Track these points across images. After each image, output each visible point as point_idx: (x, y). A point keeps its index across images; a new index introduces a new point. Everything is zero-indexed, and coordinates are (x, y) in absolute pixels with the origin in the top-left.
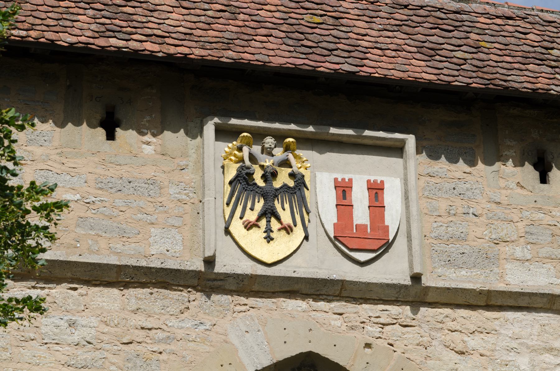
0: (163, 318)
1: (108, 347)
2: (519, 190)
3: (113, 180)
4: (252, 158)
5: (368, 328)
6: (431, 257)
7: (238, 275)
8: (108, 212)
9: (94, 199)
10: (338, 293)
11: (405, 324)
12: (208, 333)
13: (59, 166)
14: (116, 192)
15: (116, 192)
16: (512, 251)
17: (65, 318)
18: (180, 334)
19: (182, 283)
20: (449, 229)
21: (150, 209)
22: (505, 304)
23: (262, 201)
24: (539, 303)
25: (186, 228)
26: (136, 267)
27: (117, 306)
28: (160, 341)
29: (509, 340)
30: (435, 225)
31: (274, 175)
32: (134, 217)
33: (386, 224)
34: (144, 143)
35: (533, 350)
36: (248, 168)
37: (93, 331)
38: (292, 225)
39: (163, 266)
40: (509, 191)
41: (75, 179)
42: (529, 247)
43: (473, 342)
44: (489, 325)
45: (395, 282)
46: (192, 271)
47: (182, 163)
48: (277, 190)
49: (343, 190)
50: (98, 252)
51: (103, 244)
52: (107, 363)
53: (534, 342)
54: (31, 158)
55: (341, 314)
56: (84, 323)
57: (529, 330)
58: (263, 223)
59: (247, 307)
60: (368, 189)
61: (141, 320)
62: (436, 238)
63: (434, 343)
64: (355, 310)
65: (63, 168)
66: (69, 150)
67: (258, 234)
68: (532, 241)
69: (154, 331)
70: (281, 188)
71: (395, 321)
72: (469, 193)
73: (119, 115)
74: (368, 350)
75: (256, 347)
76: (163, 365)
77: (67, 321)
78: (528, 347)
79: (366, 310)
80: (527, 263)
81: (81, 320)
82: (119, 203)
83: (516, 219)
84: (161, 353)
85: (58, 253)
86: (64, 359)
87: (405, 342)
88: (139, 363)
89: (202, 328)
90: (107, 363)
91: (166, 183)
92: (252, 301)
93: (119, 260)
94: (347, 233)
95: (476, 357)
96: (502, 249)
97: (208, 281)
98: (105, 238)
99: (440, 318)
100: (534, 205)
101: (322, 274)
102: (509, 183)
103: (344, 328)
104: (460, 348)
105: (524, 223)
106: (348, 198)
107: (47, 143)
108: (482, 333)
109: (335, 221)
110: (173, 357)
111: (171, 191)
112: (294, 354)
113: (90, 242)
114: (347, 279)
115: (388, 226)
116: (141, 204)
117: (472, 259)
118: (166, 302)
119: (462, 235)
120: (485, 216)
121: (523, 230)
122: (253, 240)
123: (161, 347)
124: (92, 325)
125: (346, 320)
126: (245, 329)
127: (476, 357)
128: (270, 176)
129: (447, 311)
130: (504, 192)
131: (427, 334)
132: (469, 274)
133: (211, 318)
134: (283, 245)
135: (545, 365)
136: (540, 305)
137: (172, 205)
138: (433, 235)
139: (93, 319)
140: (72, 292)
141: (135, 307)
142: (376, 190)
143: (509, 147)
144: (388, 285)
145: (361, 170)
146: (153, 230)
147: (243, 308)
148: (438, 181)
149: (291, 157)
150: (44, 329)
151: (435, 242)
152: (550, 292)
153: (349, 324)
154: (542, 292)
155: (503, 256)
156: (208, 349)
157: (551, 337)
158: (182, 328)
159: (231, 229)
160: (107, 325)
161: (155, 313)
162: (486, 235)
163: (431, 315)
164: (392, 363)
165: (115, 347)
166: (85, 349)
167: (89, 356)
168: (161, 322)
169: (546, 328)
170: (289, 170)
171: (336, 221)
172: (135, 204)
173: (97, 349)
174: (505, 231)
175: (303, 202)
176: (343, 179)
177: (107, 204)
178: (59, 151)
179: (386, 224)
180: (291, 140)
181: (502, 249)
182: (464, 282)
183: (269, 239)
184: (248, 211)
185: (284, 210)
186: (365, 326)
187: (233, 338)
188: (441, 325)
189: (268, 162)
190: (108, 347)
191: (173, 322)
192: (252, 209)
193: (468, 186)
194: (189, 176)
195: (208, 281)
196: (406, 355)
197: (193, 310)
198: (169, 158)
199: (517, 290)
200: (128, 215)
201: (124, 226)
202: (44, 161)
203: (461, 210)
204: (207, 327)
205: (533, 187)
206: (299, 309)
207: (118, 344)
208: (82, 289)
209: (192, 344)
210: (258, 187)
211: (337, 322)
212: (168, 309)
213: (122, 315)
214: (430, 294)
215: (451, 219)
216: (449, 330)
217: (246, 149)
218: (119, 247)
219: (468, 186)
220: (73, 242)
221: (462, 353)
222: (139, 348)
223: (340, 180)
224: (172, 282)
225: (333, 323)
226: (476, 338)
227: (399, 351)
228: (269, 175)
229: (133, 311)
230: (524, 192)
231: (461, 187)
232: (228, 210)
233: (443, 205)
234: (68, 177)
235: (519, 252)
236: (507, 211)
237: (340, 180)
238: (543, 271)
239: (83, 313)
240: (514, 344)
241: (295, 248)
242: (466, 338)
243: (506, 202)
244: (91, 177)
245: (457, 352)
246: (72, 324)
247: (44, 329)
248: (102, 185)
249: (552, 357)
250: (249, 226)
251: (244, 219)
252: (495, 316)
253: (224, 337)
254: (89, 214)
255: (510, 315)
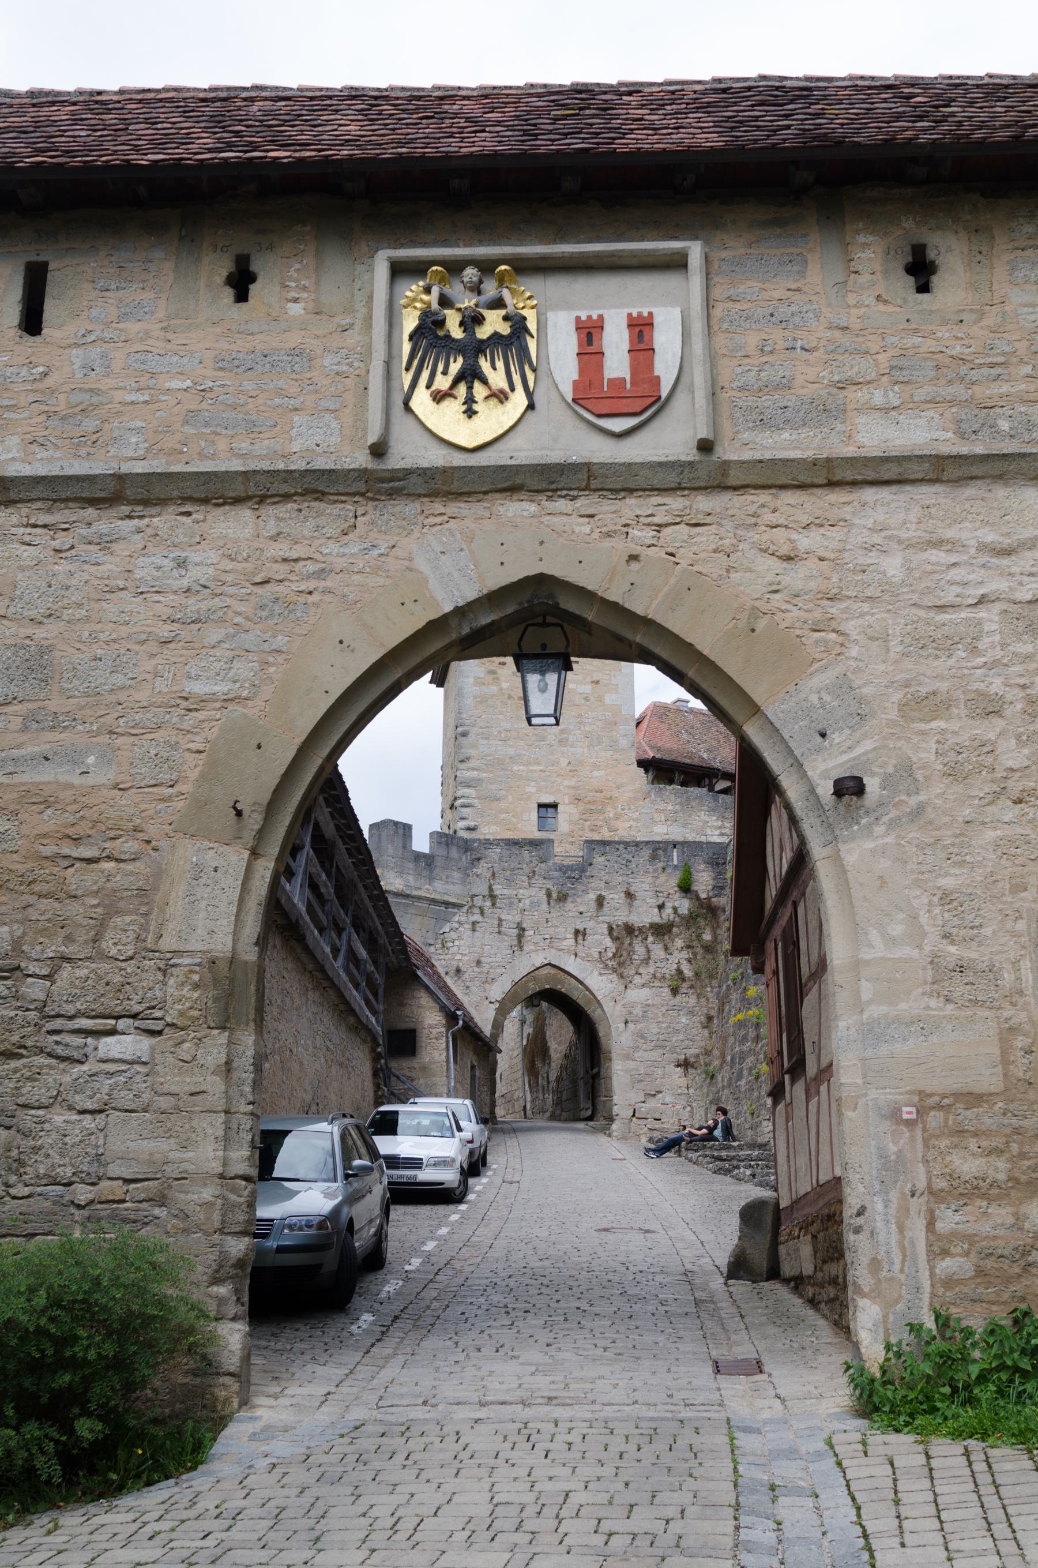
0: (316, 543)
1: (231, 590)
2: (881, 307)
3: (240, 355)
4: (445, 302)
5: (635, 532)
6: (732, 417)
7: (425, 470)
8: (230, 400)
9: (211, 384)
10: (584, 484)
11: (693, 521)
12: (383, 559)
13: (163, 345)
14: (245, 372)
15: (245, 372)
16: (868, 397)
17: (172, 555)
18: (340, 563)
19: (342, 490)
20: (762, 374)
21: (294, 390)
22: (860, 478)
23: (460, 360)
24: (918, 471)
25: (347, 411)
26: (268, 472)
27: (248, 532)
28: (309, 576)
29: (868, 533)
30: (739, 370)
31: (478, 320)
32: (269, 403)
33: (656, 373)
34: (290, 301)
35: (909, 545)
36: (436, 314)
37: (211, 571)
38: (508, 390)
39: (308, 467)
40: (863, 310)
41: (185, 360)
42: (896, 388)
43: (804, 541)
44: (833, 514)
45: (671, 458)
46: (354, 470)
47: (343, 322)
48: (482, 341)
49: (589, 333)
50: (213, 457)
51: (222, 445)
52: (230, 614)
53: (911, 534)
54: (123, 338)
55: (592, 516)
56: (198, 559)
57: (902, 516)
58: (462, 390)
59: (445, 518)
60: (629, 326)
61: (281, 549)
62: (741, 389)
63: (741, 546)
64: (613, 508)
65: (169, 346)
66: (179, 321)
67: (454, 407)
68: (901, 379)
69: (302, 563)
70: (489, 338)
71: (678, 520)
72: (797, 319)
73: (256, 266)
74: (634, 566)
75: (456, 574)
76: (313, 610)
77: (174, 560)
78: (900, 542)
79: (632, 506)
80: (893, 413)
81: (194, 556)
82: (249, 386)
83: (874, 348)
84: (310, 593)
85: (155, 462)
86: (166, 612)
87: (695, 549)
88: (277, 609)
89: (375, 552)
90: (230, 614)
91: (319, 352)
92: (454, 508)
93: (244, 465)
94: (594, 393)
95: (812, 563)
96: (851, 395)
97: (381, 483)
98: (226, 436)
99: (752, 509)
100: (906, 325)
101: (555, 457)
102: (864, 297)
103: (596, 535)
104: (784, 550)
105: (889, 354)
106: (595, 342)
107: (148, 316)
108: (822, 526)
109: (576, 377)
110: (328, 598)
111: (327, 362)
112: (515, 579)
113: (203, 444)
114: (595, 461)
115: (658, 378)
116: (281, 384)
117: (801, 414)
118: (322, 521)
119: (784, 381)
120: (822, 350)
121: (887, 365)
122: (447, 420)
123: (311, 585)
124: (209, 561)
125: (599, 524)
126: (439, 548)
127: (812, 563)
128: (472, 320)
129: (763, 497)
130: (854, 312)
131: (731, 535)
132: (794, 437)
133: (388, 537)
134: (492, 420)
135: (930, 567)
136: (920, 476)
137: (326, 382)
138: (737, 384)
139: (212, 554)
140: (184, 519)
141: (273, 532)
142: (641, 329)
143: (865, 246)
144: (661, 464)
145: (614, 302)
146: (296, 418)
147: (438, 520)
148: (745, 306)
149: (506, 294)
150: (138, 574)
151: (738, 395)
152: (934, 452)
153: (604, 530)
154: (920, 453)
155: (852, 406)
156: (381, 581)
157: (940, 524)
158: (344, 555)
159: (414, 404)
160: (233, 560)
161: (304, 537)
162: (823, 377)
163: (737, 505)
164: (673, 581)
165: (243, 591)
166: (199, 597)
167: (203, 606)
168: (313, 549)
169: (933, 510)
170: (503, 312)
171: (576, 377)
172: (271, 386)
173: (216, 595)
174: (856, 369)
175: (524, 354)
176: (589, 317)
177: (230, 390)
178: (164, 324)
179: (656, 373)
180: (503, 267)
181: (851, 395)
182: (786, 449)
183: (470, 413)
184: (439, 376)
185: (495, 369)
186: (630, 530)
187: (422, 564)
188: (753, 520)
189: (468, 302)
190: (231, 590)
191: (332, 548)
192: (445, 373)
193: (794, 308)
194: (353, 338)
195: (381, 483)
196: (695, 568)
197: (361, 528)
198: (325, 317)
199: (875, 454)
200: (260, 401)
201: (254, 417)
202: (142, 340)
203: (781, 345)
204: (382, 551)
205: (905, 300)
206: (525, 514)
207: (247, 584)
208: (199, 512)
209: (356, 578)
210: (454, 340)
211: (584, 528)
212: (324, 531)
213: (256, 544)
214: (732, 473)
215: (765, 359)
216: (767, 526)
217: (435, 290)
218: (244, 446)
219: (794, 308)
220: (177, 446)
221: (789, 559)
222: (280, 588)
223: (584, 318)
224: (327, 490)
225: (577, 529)
226: (812, 534)
227: (684, 563)
228: (468, 321)
229: (271, 538)
230: (890, 308)
231: (783, 311)
232: (407, 378)
233: (752, 340)
234: (175, 359)
235: (878, 398)
236: (861, 339)
237: (584, 318)
238: (922, 422)
239: (199, 547)
240: (877, 539)
241: (511, 423)
242: (794, 536)
243: (858, 326)
244: (210, 354)
245: (780, 557)
246: (182, 564)
247: (138, 574)
248: (223, 364)
249: (943, 554)
250: (439, 397)
251: (433, 388)
252: (843, 500)
253: (407, 563)
254: (204, 405)
255: (870, 494)
